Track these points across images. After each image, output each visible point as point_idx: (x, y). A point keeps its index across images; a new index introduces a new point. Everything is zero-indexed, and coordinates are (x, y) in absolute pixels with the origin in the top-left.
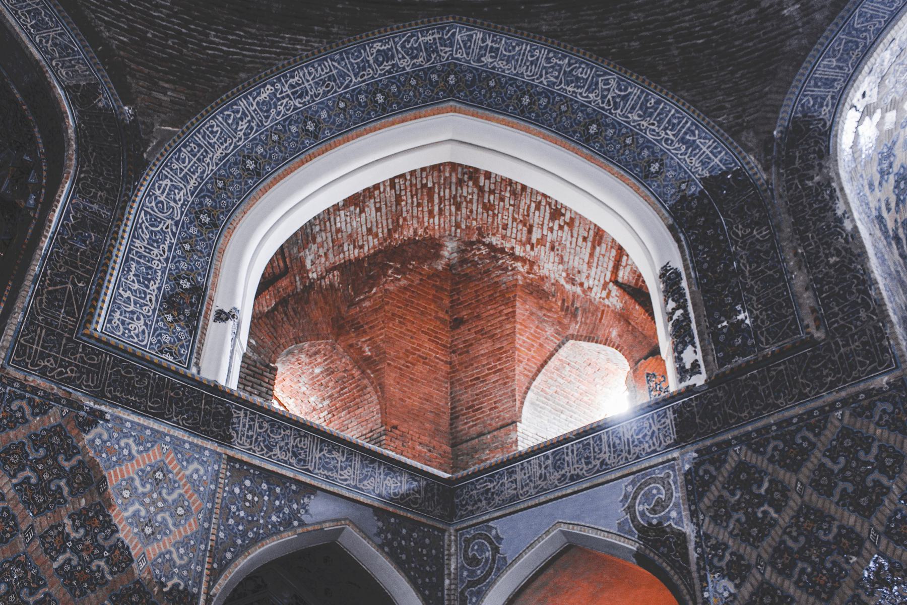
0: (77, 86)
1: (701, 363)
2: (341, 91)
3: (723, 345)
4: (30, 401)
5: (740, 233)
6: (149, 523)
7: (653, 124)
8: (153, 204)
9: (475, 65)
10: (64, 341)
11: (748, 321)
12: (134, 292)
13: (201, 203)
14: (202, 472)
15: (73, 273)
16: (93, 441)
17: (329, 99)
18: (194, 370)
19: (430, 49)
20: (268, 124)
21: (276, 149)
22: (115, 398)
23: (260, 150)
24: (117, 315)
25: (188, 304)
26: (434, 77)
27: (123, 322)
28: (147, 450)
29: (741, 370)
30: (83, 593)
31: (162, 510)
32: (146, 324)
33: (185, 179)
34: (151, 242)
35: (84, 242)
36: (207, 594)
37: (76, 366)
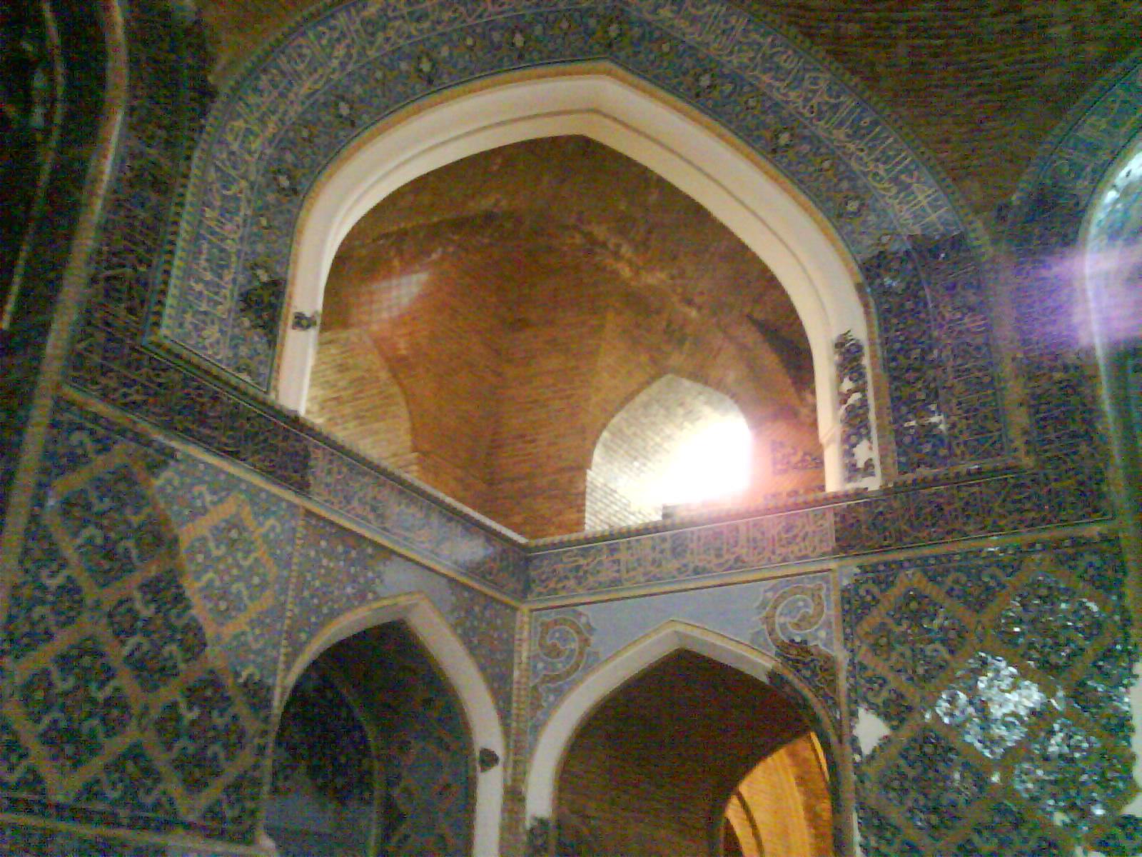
1: (876, 462)
2: (470, 21)
3: (909, 448)
4: (92, 432)
5: (947, 315)
7: (862, 150)
8: (224, 156)
9: (649, 17)
10: (127, 351)
11: (942, 427)
12: (207, 283)
13: (281, 160)
14: (278, 530)
15: (132, 251)
16: (162, 489)
17: (455, 30)
18: (272, 396)
20: (372, 53)
21: (379, 91)
22: (186, 430)
24: (188, 317)
25: (264, 305)
26: (592, 22)
27: (196, 326)
28: (221, 501)
29: (926, 483)
30: (156, 688)
32: (221, 331)
33: (262, 120)
34: (224, 211)
35: (143, 205)
37: (142, 385)
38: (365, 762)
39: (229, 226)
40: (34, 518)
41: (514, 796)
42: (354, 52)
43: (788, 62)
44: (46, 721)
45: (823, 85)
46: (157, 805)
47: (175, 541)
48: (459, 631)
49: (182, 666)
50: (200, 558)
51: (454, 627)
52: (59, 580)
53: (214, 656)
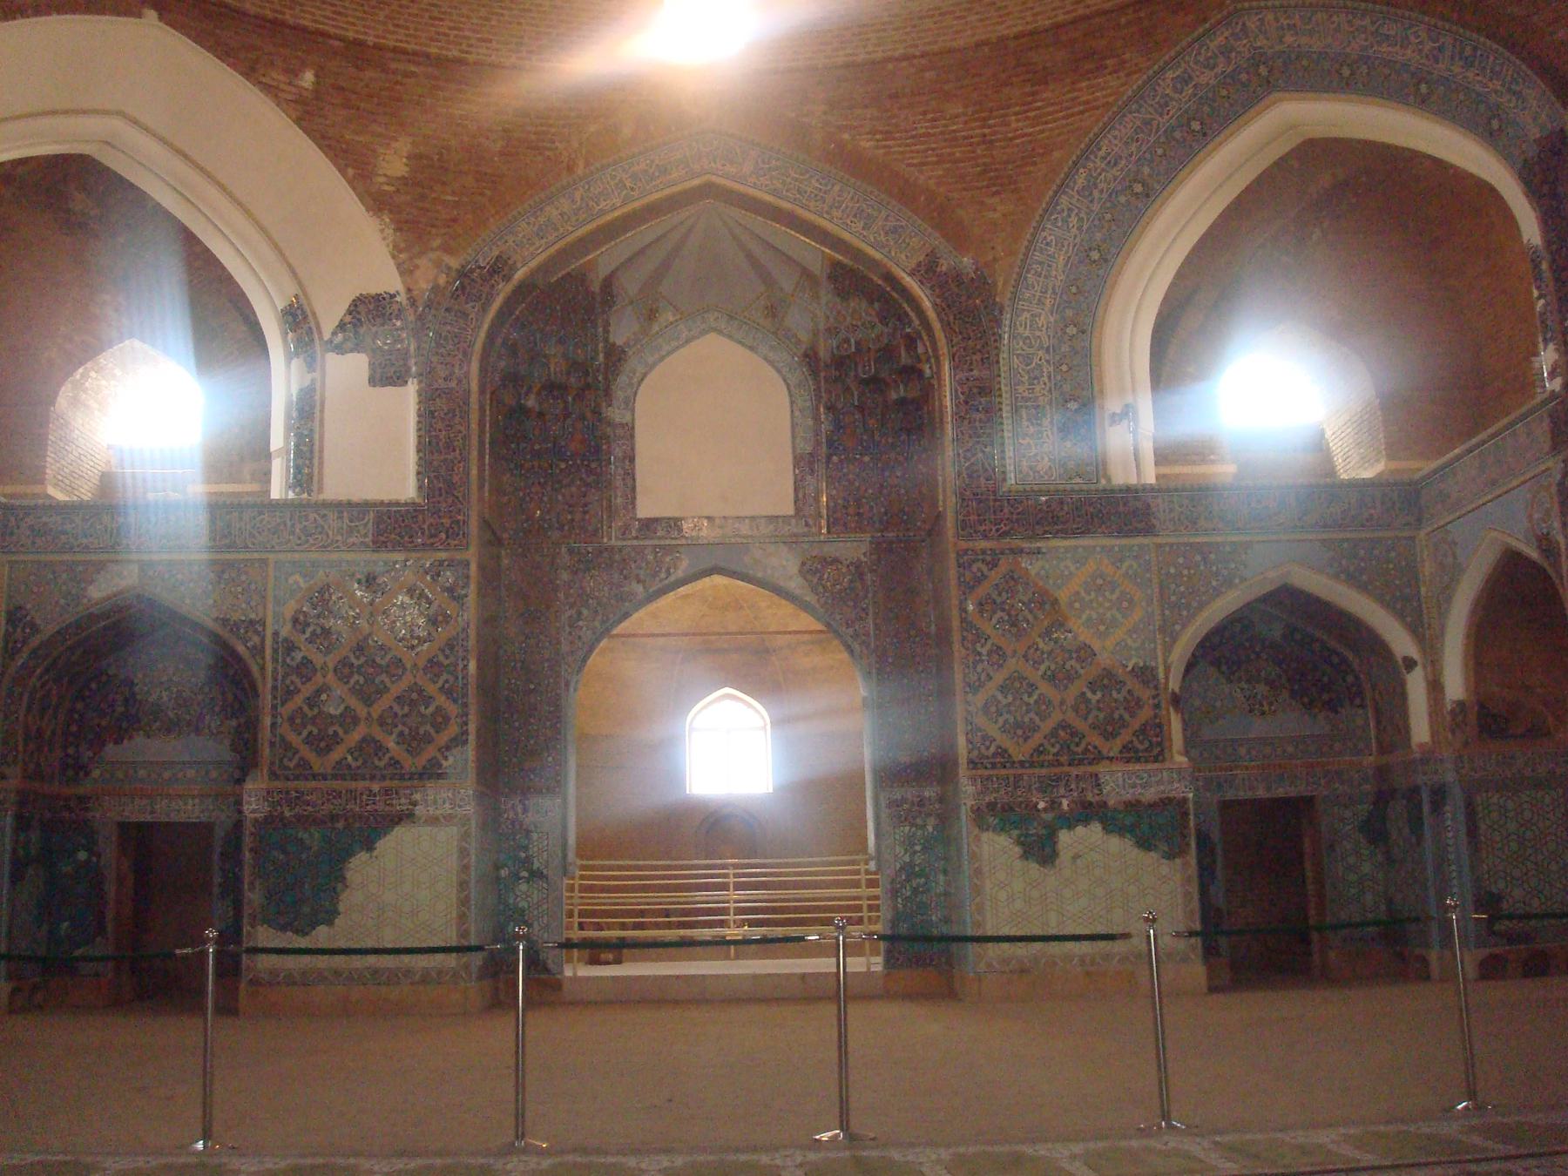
0: (919, 264)
6: (1102, 622)
9: (1278, 48)
18: (1103, 482)
19: (1226, 51)
20: (1096, 207)
23: (1098, 236)
26: (1244, 77)
30: (1066, 687)
31: (1110, 609)
36: (1165, 662)
38: (1350, 679)
39: (1038, 388)
40: (963, 620)
41: (1435, 687)
42: (1082, 215)
43: (1392, 29)
44: (1001, 720)
45: (1424, 35)
46: (1086, 750)
47: (1055, 602)
48: (1343, 576)
49: (1082, 672)
50: (1077, 605)
51: (1336, 577)
52: (988, 646)
53: (1104, 659)
